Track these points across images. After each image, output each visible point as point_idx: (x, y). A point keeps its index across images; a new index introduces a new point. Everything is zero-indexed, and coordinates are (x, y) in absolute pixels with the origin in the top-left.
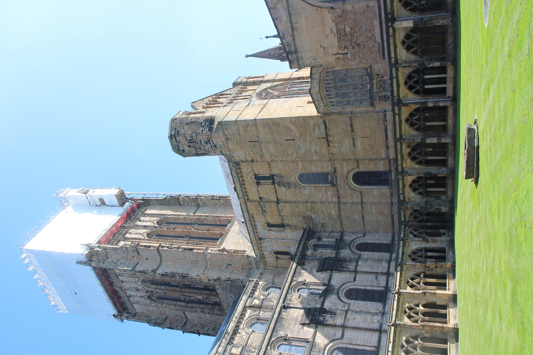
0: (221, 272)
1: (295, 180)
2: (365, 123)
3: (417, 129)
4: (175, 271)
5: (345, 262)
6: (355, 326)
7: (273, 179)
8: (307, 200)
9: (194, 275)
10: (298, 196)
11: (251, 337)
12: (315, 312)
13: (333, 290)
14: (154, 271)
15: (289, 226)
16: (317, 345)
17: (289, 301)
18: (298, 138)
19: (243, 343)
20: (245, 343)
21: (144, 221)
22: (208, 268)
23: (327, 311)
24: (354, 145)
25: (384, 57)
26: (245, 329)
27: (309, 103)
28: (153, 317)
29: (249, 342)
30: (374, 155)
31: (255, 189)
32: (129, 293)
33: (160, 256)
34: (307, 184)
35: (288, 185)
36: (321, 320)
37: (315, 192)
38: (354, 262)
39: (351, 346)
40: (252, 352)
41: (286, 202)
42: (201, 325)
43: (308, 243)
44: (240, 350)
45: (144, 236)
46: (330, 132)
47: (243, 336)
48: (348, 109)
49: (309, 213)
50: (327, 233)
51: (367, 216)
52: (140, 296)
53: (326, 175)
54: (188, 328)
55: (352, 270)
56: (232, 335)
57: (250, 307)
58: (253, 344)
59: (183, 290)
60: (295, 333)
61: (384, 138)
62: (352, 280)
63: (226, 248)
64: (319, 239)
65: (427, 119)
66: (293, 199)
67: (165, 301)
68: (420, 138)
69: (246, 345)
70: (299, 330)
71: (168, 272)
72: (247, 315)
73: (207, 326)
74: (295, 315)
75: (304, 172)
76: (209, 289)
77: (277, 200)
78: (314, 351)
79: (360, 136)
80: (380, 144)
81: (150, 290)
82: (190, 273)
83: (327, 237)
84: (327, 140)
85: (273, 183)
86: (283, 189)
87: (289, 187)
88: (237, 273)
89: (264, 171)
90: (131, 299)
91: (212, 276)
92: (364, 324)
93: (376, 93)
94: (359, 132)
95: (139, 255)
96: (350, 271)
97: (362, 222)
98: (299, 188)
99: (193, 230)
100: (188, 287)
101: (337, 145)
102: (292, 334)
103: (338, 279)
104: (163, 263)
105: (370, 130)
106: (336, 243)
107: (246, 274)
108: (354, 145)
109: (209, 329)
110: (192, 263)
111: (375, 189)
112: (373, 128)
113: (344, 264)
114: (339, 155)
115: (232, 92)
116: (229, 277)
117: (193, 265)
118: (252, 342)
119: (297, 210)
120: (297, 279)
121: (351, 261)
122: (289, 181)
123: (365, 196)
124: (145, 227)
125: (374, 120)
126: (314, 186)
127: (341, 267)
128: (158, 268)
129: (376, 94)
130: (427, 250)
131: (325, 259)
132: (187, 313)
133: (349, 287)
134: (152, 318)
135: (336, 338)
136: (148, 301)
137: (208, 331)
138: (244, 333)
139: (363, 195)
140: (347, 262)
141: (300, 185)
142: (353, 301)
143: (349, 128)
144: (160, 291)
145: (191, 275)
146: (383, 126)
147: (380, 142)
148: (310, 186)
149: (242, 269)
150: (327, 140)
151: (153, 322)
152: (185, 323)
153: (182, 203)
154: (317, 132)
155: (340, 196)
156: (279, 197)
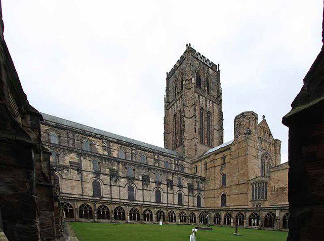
14: (185, 116)
32: (175, 104)
35: (221, 170)
53: (225, 184)
65: (240, 219)
76: (181, 143)
100: (181, 131)
103: (186, 190)
115: (270, 139)
144: (178, 119)
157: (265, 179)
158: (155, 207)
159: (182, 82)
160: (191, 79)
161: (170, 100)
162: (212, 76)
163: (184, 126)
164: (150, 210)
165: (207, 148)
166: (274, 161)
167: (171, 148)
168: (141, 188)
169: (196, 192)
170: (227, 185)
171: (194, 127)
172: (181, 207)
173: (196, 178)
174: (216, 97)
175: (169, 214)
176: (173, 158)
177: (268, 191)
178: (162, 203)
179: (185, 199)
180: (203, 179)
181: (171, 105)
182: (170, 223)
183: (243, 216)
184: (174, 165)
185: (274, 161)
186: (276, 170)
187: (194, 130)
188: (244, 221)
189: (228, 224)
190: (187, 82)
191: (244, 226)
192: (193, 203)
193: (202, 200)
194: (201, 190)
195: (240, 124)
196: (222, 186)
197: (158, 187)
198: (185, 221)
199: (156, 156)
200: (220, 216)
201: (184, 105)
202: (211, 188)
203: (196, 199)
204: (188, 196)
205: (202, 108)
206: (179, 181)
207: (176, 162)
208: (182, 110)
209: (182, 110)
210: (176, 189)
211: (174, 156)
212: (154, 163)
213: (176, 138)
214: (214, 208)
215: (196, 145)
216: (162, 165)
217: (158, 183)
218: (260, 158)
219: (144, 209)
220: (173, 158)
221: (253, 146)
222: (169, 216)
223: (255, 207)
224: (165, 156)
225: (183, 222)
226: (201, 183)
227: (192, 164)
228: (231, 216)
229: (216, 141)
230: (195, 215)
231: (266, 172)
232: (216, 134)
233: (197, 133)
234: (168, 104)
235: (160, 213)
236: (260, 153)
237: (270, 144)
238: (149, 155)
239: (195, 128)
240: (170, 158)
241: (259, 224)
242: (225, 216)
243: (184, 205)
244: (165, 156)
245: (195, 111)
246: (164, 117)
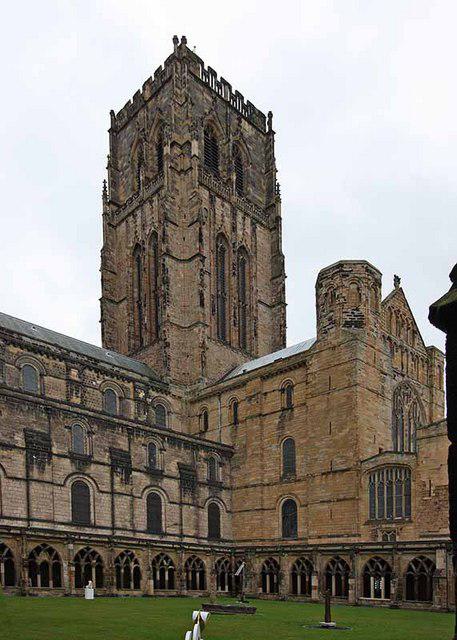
3: (328, 568)
4: (171, 283)
7: (287, 409)
9: (168, 311)
19: (87, 382)
21: (244, 225)
24: (324, 502)
25: (421, 537)
27: (380, 449)
28: (113, 254)
31: (276, 387)
35: (281, 427)
41: (261, 425)
44: (77, 379)
46: (337, 475)
48: (366, 496)
49: (249, 452)
52: (136, 232)
57: (135, 387)
59: (152, 295)
65: (338, 577)
66: (266, 434)
67: (136, 270)
68: (318, 570)
75: (297, 445)
81: (146, 246)
84: (329, 473)
85: (283, 409)
86: (277, 421)
87: (278, 429)
89: (298, 395)
94: (336, 506)
99: (232, 302)
108: (324, 502)
115: (416, 346)
143: (342, 497)
144: (147, 260)
150: (329, 473)
153: (275, 281)
154: (339, 461)
157: (404, 459)
158: (69, 538)
159: (160, 149)
160: (188, 143)
161: (123, 199)
162: (251, 143)
163: (166, 282)
164: (51, 551)
165: (239, 357)
166: (427, 409)
167: (125, 348)
168: (21, 474)
169: (205, 493)
170: (301, 472)
171: (196, 288)
172: (157, 538)
173: (203, 446)
174: (263, 206)
175: (117, 561)
176: (130, 380)
177: (413, 495)
178: (95, 527)
179: (169, 513)
180: (227, 453)
181: (123, 214)
182: (121, 593)
183: (347, 568)
184: (132, 404)
185: (427, 409)
186: (433, 433)
187: (198, 300)
188: (350, 581)
189: (303, 592)
190: (177, 151)
191: (351, 599)
192: (197, 527)
193: (224, 519)
194: (221, 487)
195: (333, 296)
196: (285, 476)
197: (80, 471)
198: (171, 586)
199: (74, 373)
200: (278, 567)
201: (166, 219)
202: (251, 480)
203: (204, 514)
204: (181, 504)
205: (222, 235)
206: (152, 455)
207: (142, 395)
208: (160, 233)
209: (160, 233)
210: (141, 479)
211: (135, 376)
212: (69, 395)
213: (141, 319)
214: (260, 544)
215: (203, 346)
216: (95, 401)
217: (82, 461)
218: (390, 396)
219: (31, 546)
220: (130, 380)
221: (371, 362)
222: (118, 568)
223: (380, 540)
224: (106, 373)
225: (162, 587)
226: (221, 464)
227: (192, 402)
228: (312, 568)
229: (264, 339)
230: (202, 566)
231: (406, 439)
232: (264, 316)
233: (207, 310)
234: (116, 210)
235: (88, 560)
236: (390, 384)
237: (415, 358)
239: (201, 295)
240: (120, 382)
241: (393, 591)
242: (294, 568)
243: (166, 534)
244: (106, 373)
245: (201, 241)
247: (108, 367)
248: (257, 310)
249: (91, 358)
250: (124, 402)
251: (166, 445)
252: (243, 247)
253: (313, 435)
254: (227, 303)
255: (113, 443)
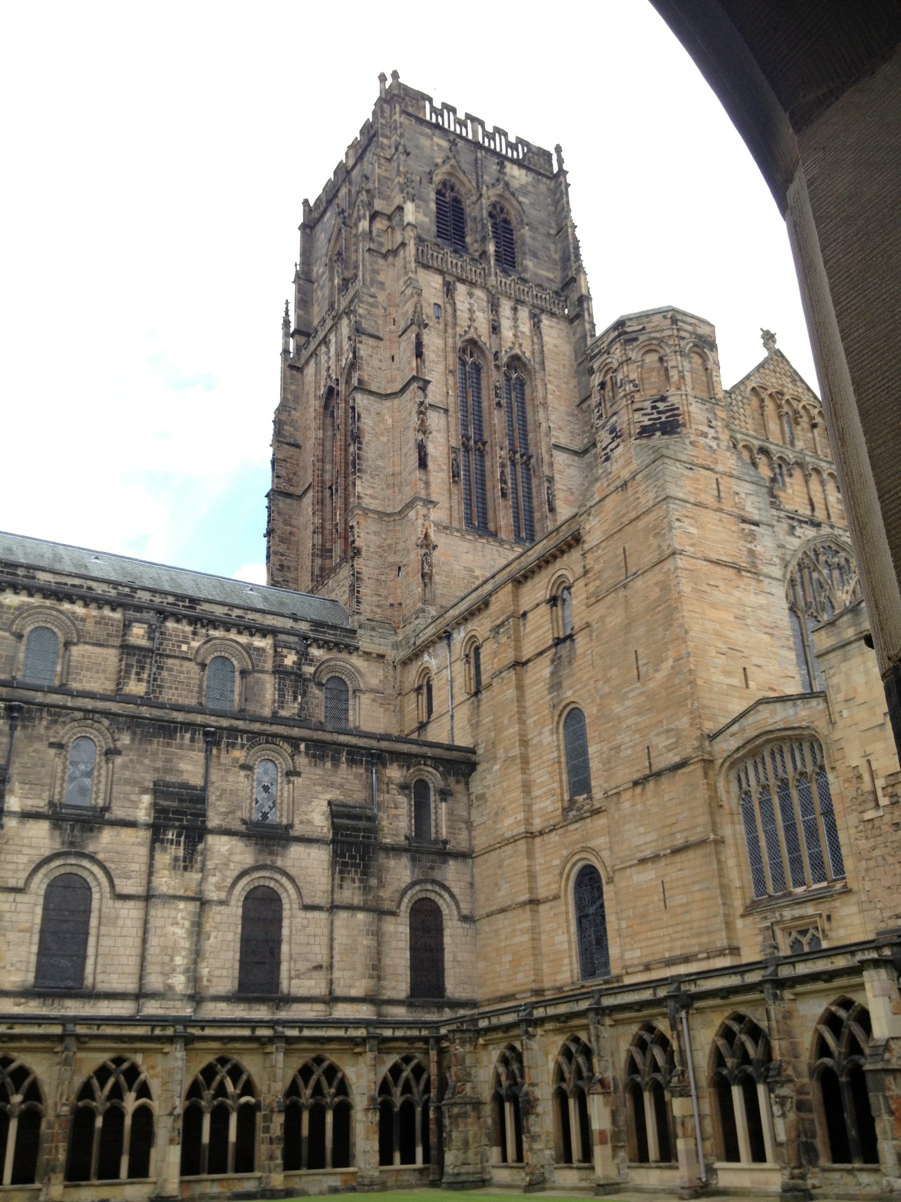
0: (376, 553)
1: (568, 701)
2: (697, 887)
4: (366, 438)
5: (364, 873)
6: (149, 926)
8: (530, 743)
9: (359, 489)
10: (536, 718)
11: (186, 663)
12: (191, 814)
13: (271, 853)
15: (478, 706)
16: (91, 835)
17: (228, 745)
18: (643, 689)
19: (168, 647)
20: (168, 652)
21: (515, 320)
22: (385, 519)
23: (195, 846)
24: (643, 861)
26: (208, 645)
29: (170, 661)
30: (628, 927)
33: (403, 390)
34: (565, 737)
35: (555, 685)
36: (164, 834)
37: (546, 764)
38: (362, 898)
39: (94, 922)
40: (138, 674)
41: (520, 687)
42: (291, 533)
43: (425, 764)
44: (144, 643)
45: (466, 332)
47: (188, 643)
49: (501, 753)
50: (465, 814)
51: (506, 923)
52: (329, 368)
54: (277, 505)
55: (337, 896)
56: (185, 616)
57: (275, 646)
58: (165, 674)
60: (127, 774)
61: (667, 955)
62: (308, 901)
63: (436, 553)
64: (445, 794)
66: (528, 703)
69: (161, 655)
70: (136, 783)
71: (363, 420)
72: (259, 642)
73: (288, 548)
74: (183, 766)
77: (524, 660)
78: (72, 830)
79: (665, 875)
80: (653, 942)
82: (366, 477)
83: (451, 813)
86: (547, 672)
88: (379, 595)
90: (323, 349)
91: (362, 535)
92: (158, 950)
93: (781, 915)
95: (400, 336)
96: (332, 892)
97: (494, 908)
98: (552, 718)
99: (497, 456)
101: (639, 807)
102: (125, 767)
104: (388, 403)
105: (682, 905)
106: (436, 841)
107: (377, 617)
108: (643, 861)
109: (282, 555)
110: (393, 475)
111: (569, 937)
112: (687, 918)
113: (356, 872)
114: (616, 817)
116: (365, 576)
117: (390, 478)
118: (170, 670)
119: (506, 721)
120: (303, 754)
121: (366, 889)
122: (565, 684)
123: (551, 908)
124: (495, 329)
125: (708, 918)
126: (559, 757)
127: (345, 864)
128: (371, 393)
129: (779, 918)
130: (344, 1113)
131: (372, 819)
132: (310, 494)
133: (284, 896)
134: (293, 412)
135: (117, 881)
136: (322, 390)
137: (276, 553)
138: (195, 644)
139: (553, 903)
140: (361, 881)
141: (560, 716)
142: (240, 911)
145: (358, 482)
146: (696, 949)
147: (658, 940)
148: (558, 746)
149: (392, 605)
150: (646, 779)
151: (284, 417)
152: (289, 495)
153: (584, 406)
155: (546, 837)
156: (530, 664)
171: (412, 436)
175: (86, 1091)
181: (312, 347)
199: (138, 634)
207: (290, 659)
215: (427, 544)
220: (264, 632)
224: (213, 623)
227: (405, 663)
238: (90, 626)
240: (243, 639)
244: (213, 623)
246: (280, 411)
247: (219, 611)
248: (551, 465)
249: (180, 597)
250: (250, 679)
251: (302, 761)
252: (516, 358)
253: (606, 689)
254: (487, 458)
255: (167, 771)
